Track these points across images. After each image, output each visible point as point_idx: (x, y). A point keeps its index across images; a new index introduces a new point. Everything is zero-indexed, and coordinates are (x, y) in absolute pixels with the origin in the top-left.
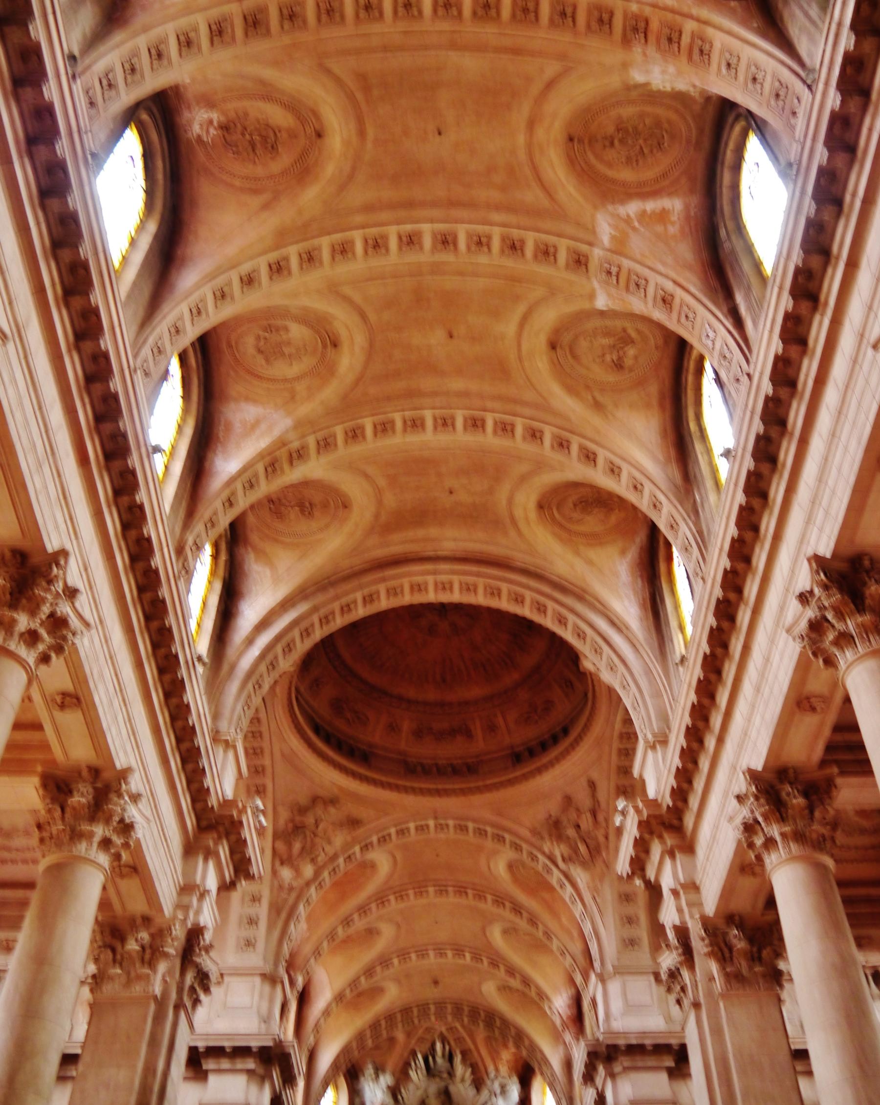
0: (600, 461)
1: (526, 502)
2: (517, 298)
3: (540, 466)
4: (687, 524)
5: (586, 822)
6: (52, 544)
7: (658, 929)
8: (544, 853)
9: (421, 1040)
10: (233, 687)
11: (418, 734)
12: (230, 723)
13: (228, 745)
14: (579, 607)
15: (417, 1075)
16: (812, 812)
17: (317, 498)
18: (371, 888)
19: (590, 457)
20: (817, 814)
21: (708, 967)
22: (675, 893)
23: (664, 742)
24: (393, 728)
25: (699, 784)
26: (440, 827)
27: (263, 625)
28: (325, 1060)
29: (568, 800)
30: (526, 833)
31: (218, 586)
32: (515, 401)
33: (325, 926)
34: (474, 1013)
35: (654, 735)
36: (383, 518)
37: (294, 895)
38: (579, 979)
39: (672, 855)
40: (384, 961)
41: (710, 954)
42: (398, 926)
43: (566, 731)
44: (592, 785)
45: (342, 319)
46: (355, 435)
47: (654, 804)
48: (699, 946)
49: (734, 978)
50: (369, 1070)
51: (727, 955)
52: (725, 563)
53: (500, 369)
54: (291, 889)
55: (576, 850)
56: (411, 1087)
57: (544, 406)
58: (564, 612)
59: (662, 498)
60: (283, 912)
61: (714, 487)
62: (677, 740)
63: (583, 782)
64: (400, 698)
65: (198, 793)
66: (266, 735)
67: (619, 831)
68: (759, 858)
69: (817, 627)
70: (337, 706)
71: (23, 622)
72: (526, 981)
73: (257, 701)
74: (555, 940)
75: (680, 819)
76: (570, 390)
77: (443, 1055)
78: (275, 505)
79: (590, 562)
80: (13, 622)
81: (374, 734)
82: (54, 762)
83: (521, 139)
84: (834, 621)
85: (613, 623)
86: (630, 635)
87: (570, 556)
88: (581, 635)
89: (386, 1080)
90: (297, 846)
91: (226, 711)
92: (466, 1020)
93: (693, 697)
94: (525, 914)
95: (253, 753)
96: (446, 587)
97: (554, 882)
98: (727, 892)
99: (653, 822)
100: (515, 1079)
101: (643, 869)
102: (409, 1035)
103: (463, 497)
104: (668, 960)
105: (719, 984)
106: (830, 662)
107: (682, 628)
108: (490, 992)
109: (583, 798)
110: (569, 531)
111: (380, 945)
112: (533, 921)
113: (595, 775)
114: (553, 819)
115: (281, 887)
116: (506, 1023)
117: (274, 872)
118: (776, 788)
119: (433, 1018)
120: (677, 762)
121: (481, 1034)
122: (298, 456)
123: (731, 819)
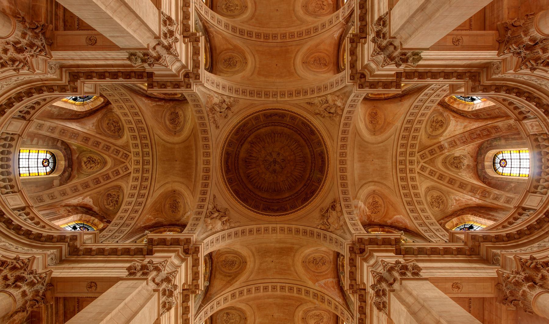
42: (294, 10)
57: (247, 302)
63: (221, 127)
64: (289, 128)
103: (269, 260)
113: (217, 131)
117: (344, 104)
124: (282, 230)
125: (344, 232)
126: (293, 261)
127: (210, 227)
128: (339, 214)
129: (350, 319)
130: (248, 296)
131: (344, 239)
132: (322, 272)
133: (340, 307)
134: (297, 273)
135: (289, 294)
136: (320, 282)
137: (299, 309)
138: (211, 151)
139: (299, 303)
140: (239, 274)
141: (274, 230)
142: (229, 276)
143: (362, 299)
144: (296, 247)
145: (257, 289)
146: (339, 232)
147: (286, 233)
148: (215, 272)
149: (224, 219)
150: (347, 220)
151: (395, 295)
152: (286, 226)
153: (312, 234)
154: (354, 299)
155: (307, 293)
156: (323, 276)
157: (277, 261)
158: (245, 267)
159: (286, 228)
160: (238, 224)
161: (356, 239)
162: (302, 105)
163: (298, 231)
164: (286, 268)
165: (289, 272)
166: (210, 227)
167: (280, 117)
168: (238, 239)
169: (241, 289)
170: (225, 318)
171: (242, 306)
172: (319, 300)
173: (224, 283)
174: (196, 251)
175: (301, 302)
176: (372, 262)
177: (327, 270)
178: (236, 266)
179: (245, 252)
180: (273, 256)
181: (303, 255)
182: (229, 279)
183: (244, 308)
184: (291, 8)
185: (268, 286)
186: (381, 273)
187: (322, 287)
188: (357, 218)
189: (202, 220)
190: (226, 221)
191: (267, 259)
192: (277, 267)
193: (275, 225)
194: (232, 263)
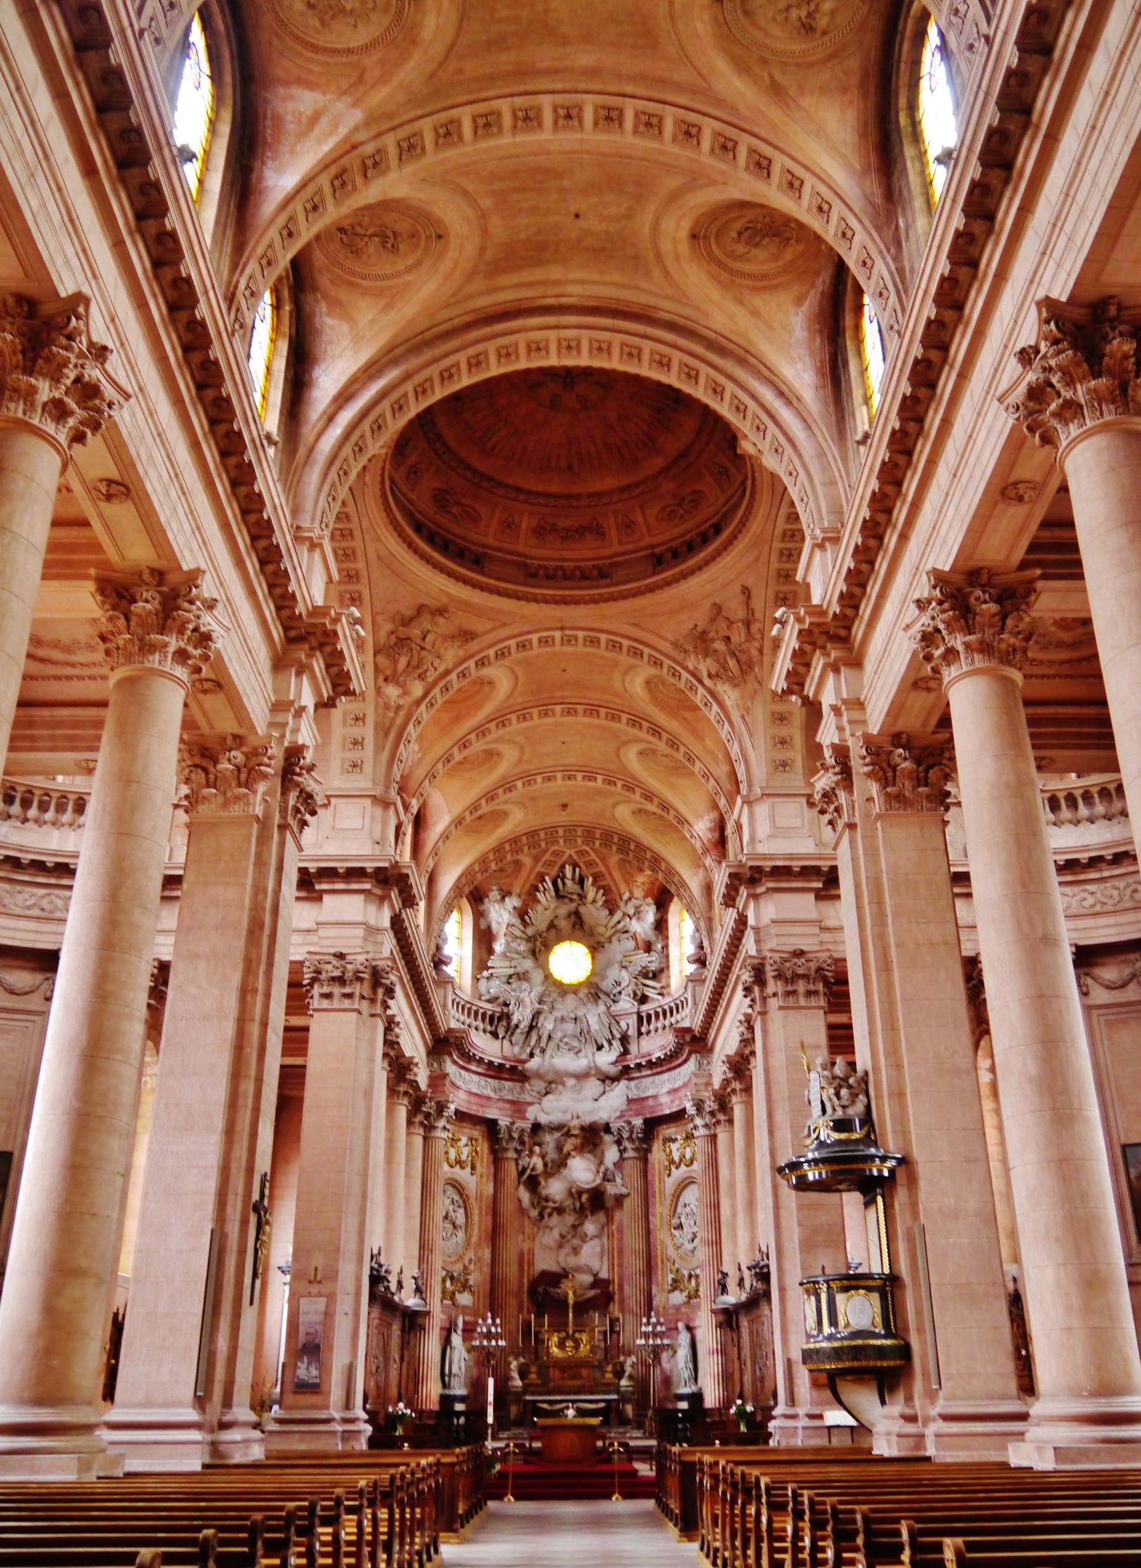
0: (776, 171)
1: (676, 229)
3: (695, 179)
4: (884, 259)
5: (738, 636)
6: (66, 287)
7: (814, 750)
8: (686, 669)
9: (549, 864)
10: (314, 475)
11: (540, 532)
12: (313, 519)
13: (314, 545)
14: (741, 373)
15: (546, 898)
16: (1004, 618)
17: (403, 226)
18: (488, 709)
19: (761, 166)
20: (1010, 622)
21: (867, 788)
22: (836, 710)
23: (836, 540)
24: (509, 525)
25: (873, 590)
26: (568, 641)
27: (343, 398)
28: (446, 883)
29: (718, 609)
30: (666, 647)
31: (284, 346)
32: (663, 82)
33: (438, 750)
34: (607, 837)
35: (824, 530)
36: (490, 254)
37: (402, 714)
38: (722, 802)
39: (837, 671)
40: (507, 786)
41: (869, 775)
42: (522, 748)
43: (718, 529)
44: (746, 592)
46: (448, 134)
47: (819, 611)
48: (859, 766)
49: (896, 800)
50: (495, 894)
51: (890, 774)
52: (930, 311)
54: (399, 708)
55: (725, 667)
56: (539, 908)
57: (704, 91)
58: (721, 379)
59: (854, 223)
60: (391, 733)
61: (924, 206)
62: (852, 537)
63: (737, 589)
64: (519, 490)
65: (284, 601)
66: (357, 533)
67: (776, 643)
68: (935, 670)
69: (1037, 394)
70: (441, 498)
71: (45, 391)
72: (665, 806)
73: (343, 493)
74: (698, 764)
75: (849, 628)
76: (742, 67)
77: (573, 879)
78: (347, 235)
79: (755, 313)
80: (33, 390)
81: (486, 534)
82: (106, 564)
84: (1058, 386)
85: (781, 394)
86: (801, 408)
87: (731, 306)
88: (741, 409)
89: (513, 902)
90: (403, 661)
91: (308, 505)
92: (597, 843)
93: (874, 485)
94: (665, 735)
95: (345, 556)
96: (572, 347)
97: (698, 700)
98: (896, 709)
99: (816, 631)
100: (650, 900)
101: (802, 685)
102: (536, 859)
104: (824, 781)
105: (877, 807)
106: (1048, 439)
107: (867, 400)
108: (624, 817)
109: (735, 607)
110: (732, 272)
111: (502, 769)
112: (673, 744)
113: (749, 581)
114: (699, 629)
115: (387, 707)
116: (641, 848)
117: (378, 690)
118: (963, 593)
119: (561, 841)
120: (849, 563)
121: (614, 858)
122: (374, 165)
123: (908, 627)
126: (485, 233)
134: (465, 193)
137: (439, 48)
138: (778, 545)
144: (473, 287)
158: (697, 222)
162: (489, 625)
164: (516, 197)
167: (554, 528)
178: (738, 225)
180: (574, 234)
181: (445, 266)
183: (721, 64)
184: (528, 750)
191: (603, 226)
192: (555, 197)
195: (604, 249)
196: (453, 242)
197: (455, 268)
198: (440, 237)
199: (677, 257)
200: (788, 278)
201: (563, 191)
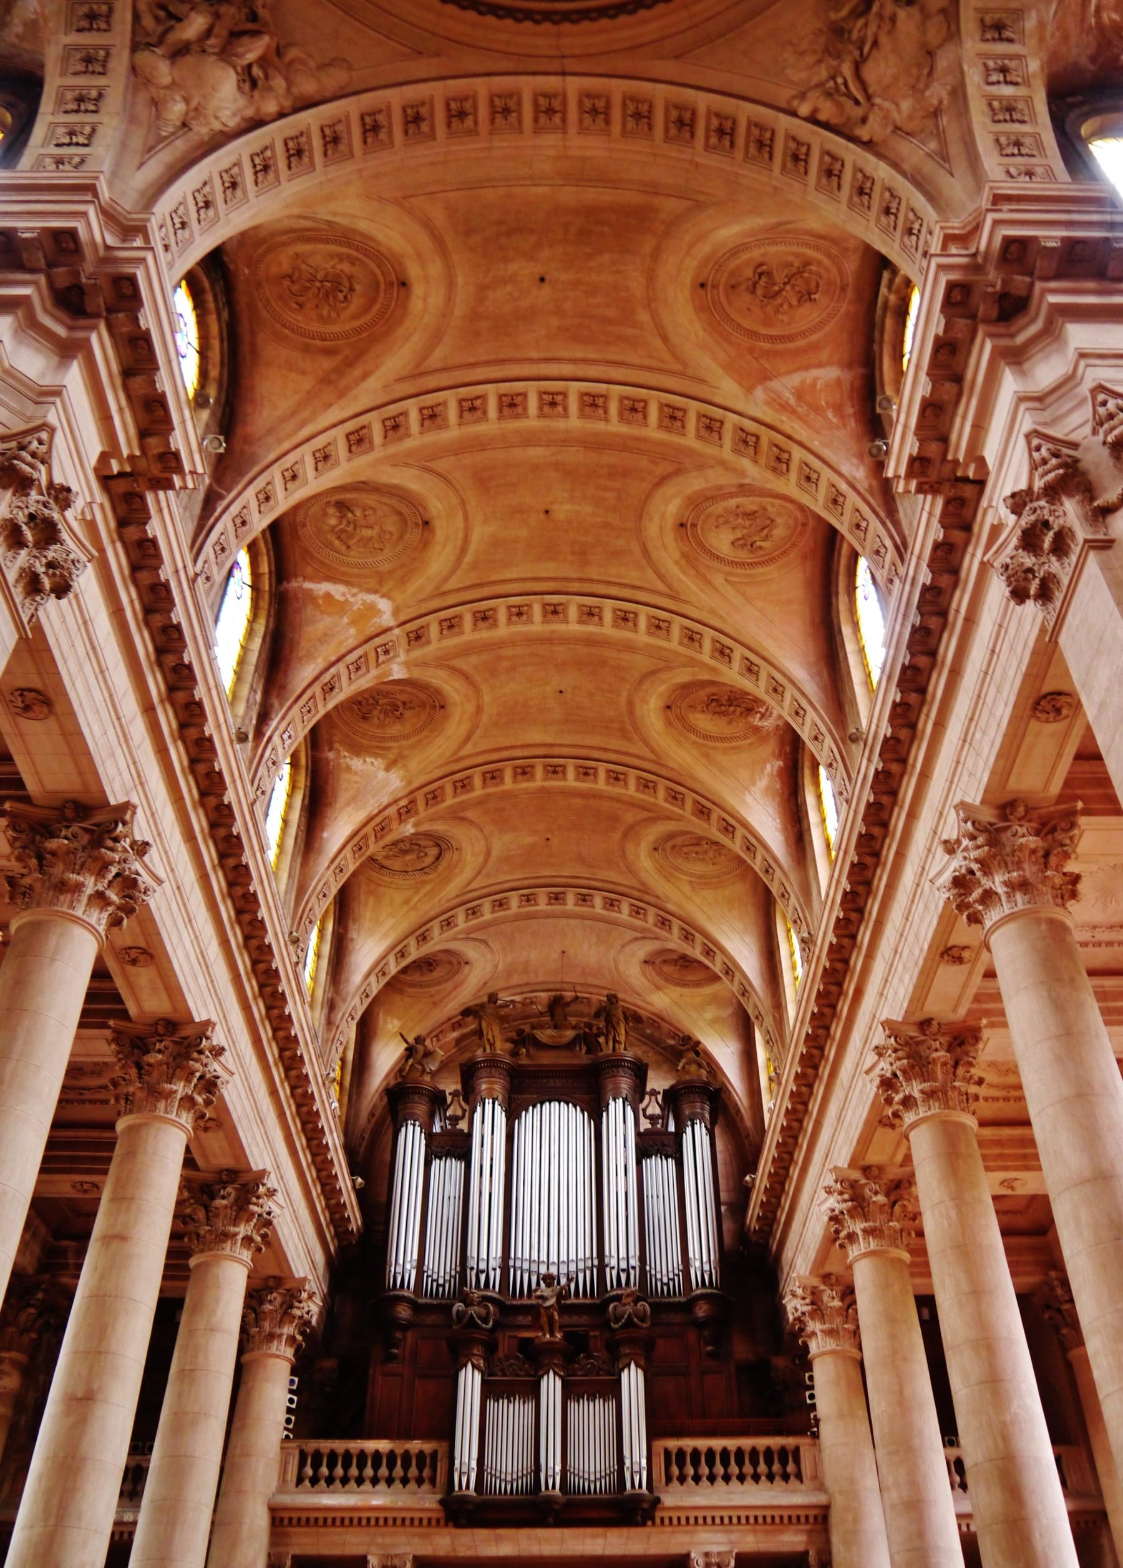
2: (475, 566)
45: (668, 552)
53: (485, 481)
57: (425, 461)
83: (487, 699)
103: (523, 269)
124: (596, 110)
125: (943, 157)
126: (651, 278)
127: (177, 109)
128: (934, 33)
129: (891, 555)
130: (431, 437)
131: (932, 198)
132: (790, 338)
133: (853, 499)
134: (665, 339)
135: (624, 429)
136: (775, 384)
137: (669, 489)
139: (661, 469)
140: (373, 340)
141: (549, 109)
142: (328, 352)
143: (960, 517)
145: (471, 408)
146: (913, 152)
147: (616, 128)
148: (253, 334)
149: (253, 51)
150: (974, 77)
151: (1106, 568)
152: (618, 88)
153: (763, 144)
154: (924, 518)
155: (709, 428)
156: (798, 352)
157: (564, 277)
159: (617, 100)
160: (335, 78)
161: (997, 242)
163: (683, 123)
164: (611, 313)
165: (629, 331)
166: (177, 109)
168: (348, 168)
169: (392, 410)
170: (333, 521)
171: (409, 479)
172: (762, 460)
173: (307, 383)
174: (121, 297)
175: (678, 464)
176: (1047, 371)
177: (822, 324)
178: (357, 302)
179: (391, 232)
180: (546, 253)
181: (704, 249)
182: (327, 363)
185: (524, 395)
186: (1075, 446)
187: (784, 407)
188: (1034, 65)
189: (120, 63)
190: (263, 61)
191: (513, 267)
193: (552, 83)
194: (334, 289)
195: (509, 233)
196: (687, 278)
197: (691, 246)
198: (702, 285)
199: (420, 257)
200: (278, 239)
201: (559, 312)
